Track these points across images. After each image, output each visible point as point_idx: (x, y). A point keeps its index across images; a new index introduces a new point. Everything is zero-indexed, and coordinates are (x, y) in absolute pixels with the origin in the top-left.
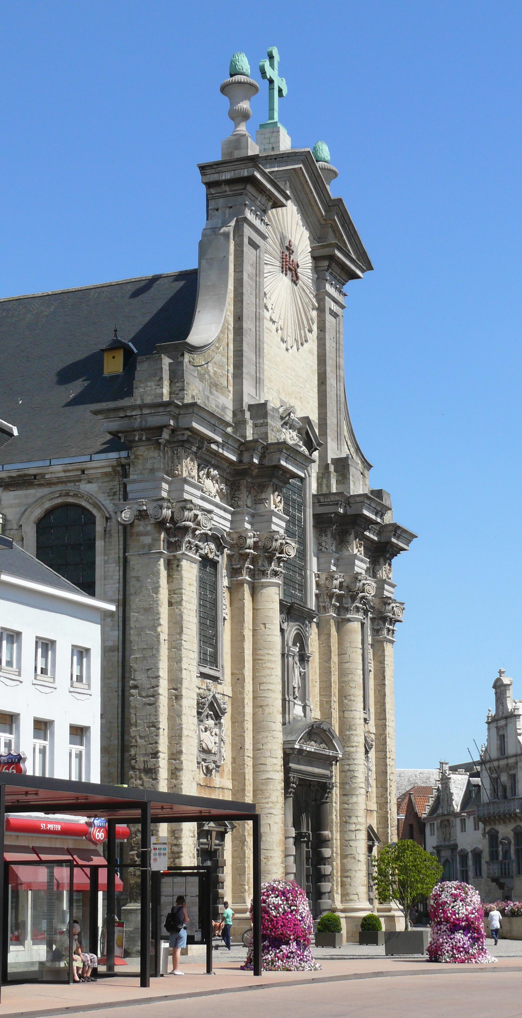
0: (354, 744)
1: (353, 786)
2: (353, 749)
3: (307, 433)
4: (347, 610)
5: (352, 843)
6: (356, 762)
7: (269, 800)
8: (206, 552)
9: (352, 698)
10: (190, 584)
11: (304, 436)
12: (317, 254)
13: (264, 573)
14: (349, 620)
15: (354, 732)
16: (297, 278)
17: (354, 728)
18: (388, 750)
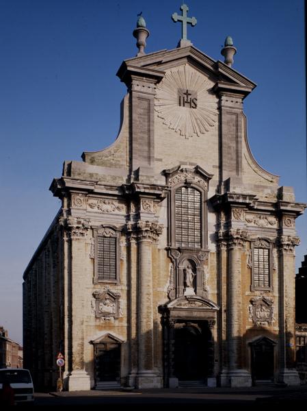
14: (232, 249)
16: (196, 105)
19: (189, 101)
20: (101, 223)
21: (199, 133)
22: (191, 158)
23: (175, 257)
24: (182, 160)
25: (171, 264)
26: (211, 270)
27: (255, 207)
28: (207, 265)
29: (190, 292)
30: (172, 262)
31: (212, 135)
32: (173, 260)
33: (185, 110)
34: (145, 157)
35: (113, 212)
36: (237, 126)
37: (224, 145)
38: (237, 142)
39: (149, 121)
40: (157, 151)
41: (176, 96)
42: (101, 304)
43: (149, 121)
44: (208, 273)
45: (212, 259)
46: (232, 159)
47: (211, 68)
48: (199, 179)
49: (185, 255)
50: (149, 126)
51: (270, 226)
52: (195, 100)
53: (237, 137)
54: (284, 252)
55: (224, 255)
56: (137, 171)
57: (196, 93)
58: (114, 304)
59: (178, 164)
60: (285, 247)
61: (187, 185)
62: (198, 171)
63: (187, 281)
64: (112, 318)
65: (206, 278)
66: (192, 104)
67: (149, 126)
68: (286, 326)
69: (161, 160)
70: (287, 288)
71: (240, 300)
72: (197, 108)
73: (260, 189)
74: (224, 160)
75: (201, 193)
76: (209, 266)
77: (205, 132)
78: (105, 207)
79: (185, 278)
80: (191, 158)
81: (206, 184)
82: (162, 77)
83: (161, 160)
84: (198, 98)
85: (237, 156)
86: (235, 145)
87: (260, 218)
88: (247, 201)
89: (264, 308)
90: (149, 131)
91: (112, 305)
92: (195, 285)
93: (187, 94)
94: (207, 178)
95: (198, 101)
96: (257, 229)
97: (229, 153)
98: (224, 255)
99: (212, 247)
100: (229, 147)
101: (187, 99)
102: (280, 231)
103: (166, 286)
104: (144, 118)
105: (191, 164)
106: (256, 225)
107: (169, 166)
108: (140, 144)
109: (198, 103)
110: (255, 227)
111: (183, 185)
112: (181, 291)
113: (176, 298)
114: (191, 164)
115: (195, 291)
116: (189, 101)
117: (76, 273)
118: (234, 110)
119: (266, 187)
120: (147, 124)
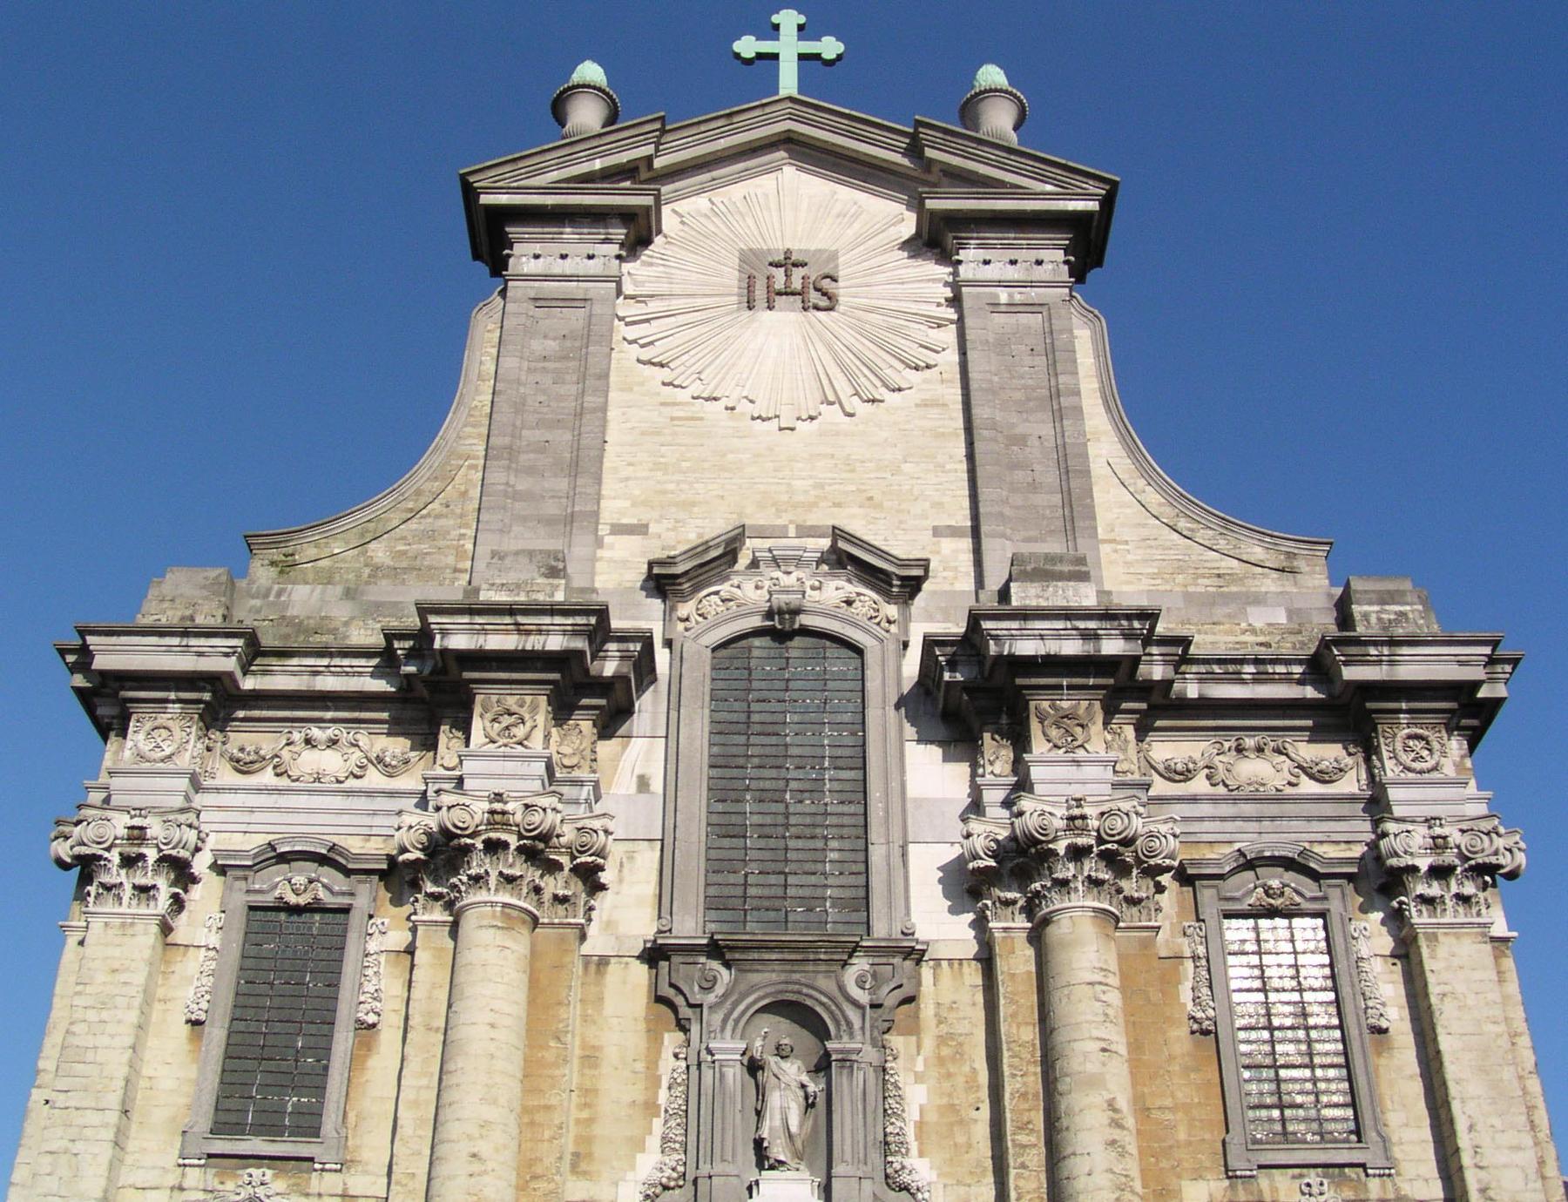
8: (277, 893)
19: (797, 284)
20: (262, 840)
21: (854, 404)
22: (812, 506)
23: (697, 997)
24: (755, 519)
25: (672, 1039)
26: (941, 1061)
27: (1192, 691)
28: (914, 1029)
30: (682, 1026)
31: (925, 404)
32: (685, 1012)
33: (785, 321)
34: (549, 522)
35: (352, 783)
36: (1051, 352)
38: (1059, 415)
44: (919, 1078)
45: (949, 994)
46: (1034, 487)
47: (905, 162)
48: (853, 589)
49: (755, 978)
51: (1308, 787)
52: (826, 284)
54: (1419, 917)
55: (1017, 961)
57: (834, 256)
60: (1421, 889)
61: (782, 627)
62: (845, 557)
65: (912, 1114)
66: (814, 297)
69: (640, 529)
70: (1484, 1138)
72: (841, 308)
73: (1219, 612)
75: (859, 651)
76: (928, 1042)
77: (882, 393)
78: (310, 761)
80: (812, 506)
81: (892, 610)
83: (640, 529)
84: (842, 273)
85: (1065, 472)
86: (1047, 430)
87: (1240, 750)
88: (1112, 646)
93: (788, 262)
94: (904, 584)
95: (841, 284)
96: (1226, 809)
98: (1017, 961)
99: (942, 927)
101: (791, 282)
102: (1376, 804)
105: (805, 531)
106: (1221, 790)
107: (678, 536)
108: (531, 471)
109: (842, 290)
110: (1214, 800)
111: (756, 622)
114: (805, 531)
118: (1033, 294)
119: (1258, 600)
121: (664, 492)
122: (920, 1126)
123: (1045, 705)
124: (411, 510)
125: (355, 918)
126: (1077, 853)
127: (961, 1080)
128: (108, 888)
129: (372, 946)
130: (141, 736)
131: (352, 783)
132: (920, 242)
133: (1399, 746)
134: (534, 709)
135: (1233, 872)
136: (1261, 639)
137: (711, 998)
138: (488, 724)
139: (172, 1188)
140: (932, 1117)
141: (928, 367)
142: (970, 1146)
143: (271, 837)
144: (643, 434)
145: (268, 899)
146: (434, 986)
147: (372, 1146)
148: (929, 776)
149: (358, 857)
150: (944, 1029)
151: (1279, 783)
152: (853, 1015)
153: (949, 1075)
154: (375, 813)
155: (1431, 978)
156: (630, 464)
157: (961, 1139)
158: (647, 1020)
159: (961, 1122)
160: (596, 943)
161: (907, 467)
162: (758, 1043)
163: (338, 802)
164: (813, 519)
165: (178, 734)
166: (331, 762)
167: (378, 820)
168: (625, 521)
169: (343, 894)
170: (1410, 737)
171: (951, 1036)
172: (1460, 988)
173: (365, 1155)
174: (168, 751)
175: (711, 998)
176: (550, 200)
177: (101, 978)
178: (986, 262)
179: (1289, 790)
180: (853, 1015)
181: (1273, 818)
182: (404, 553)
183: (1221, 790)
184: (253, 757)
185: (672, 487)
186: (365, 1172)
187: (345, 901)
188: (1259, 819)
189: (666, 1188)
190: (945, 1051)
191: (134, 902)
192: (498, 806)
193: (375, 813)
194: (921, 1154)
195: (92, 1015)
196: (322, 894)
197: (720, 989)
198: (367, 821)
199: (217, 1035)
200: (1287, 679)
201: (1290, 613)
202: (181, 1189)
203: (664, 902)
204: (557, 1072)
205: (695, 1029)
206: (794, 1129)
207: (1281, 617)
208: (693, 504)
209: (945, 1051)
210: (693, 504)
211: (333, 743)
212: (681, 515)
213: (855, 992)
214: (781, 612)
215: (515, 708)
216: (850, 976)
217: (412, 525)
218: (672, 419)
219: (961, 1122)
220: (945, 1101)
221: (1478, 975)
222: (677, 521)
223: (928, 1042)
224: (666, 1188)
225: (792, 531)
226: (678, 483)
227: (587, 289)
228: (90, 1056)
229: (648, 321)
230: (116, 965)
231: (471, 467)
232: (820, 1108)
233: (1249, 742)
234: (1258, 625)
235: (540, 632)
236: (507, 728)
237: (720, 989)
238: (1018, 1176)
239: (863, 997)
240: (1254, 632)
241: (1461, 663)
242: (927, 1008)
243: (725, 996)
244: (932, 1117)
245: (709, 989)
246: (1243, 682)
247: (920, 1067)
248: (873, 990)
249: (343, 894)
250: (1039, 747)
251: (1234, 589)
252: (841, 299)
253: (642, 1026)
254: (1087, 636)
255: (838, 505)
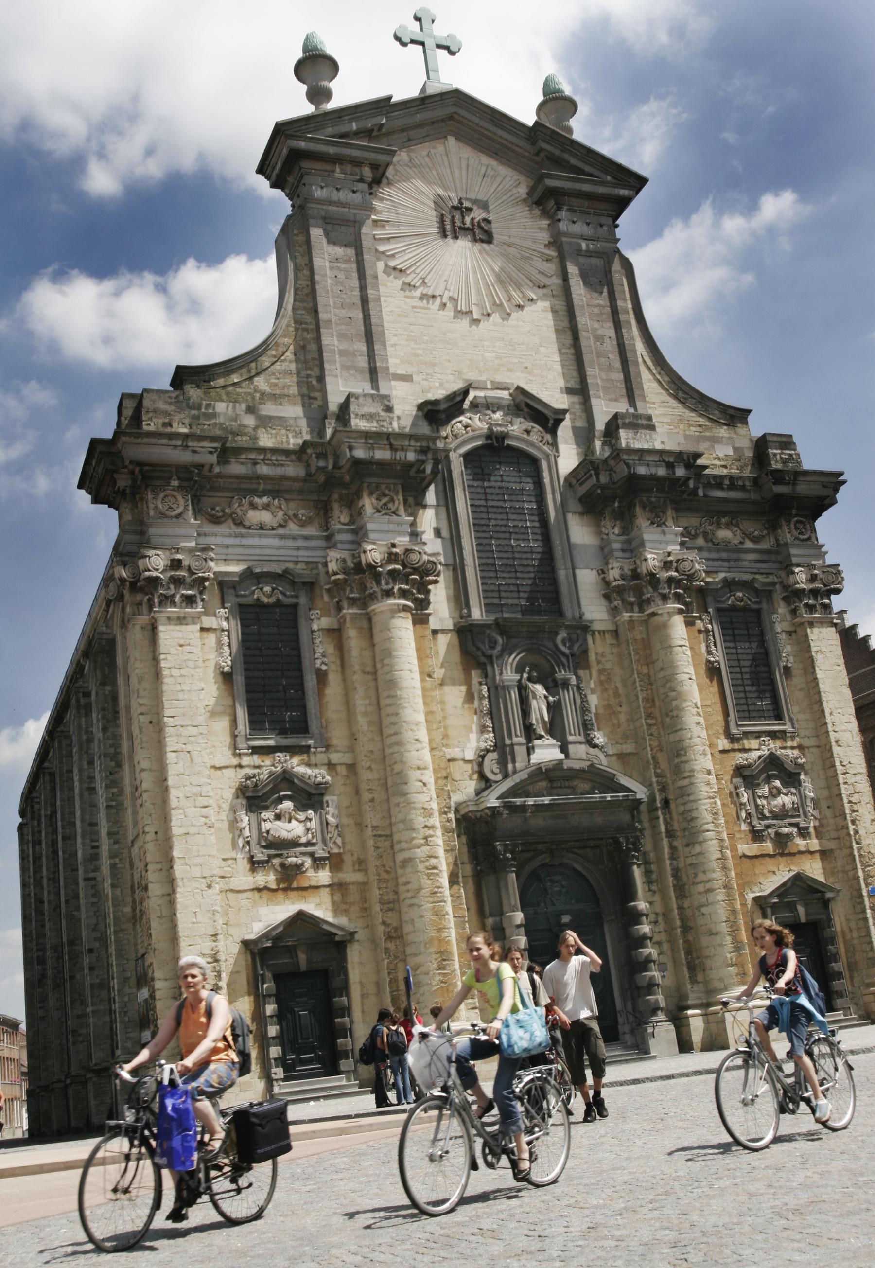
0: (686, 774)
1: (694, 830)
2: (686, 782)
3: (528, 405)
4: (649, 601)
5: (704, 910)
6: (691, 798)
7: (409, 887)
9: (675, 713)
10: (181, 646)
11: (526, 410)
12: (536, 197)
13: (372, 597)
15: (684, 759)
17: (682, 752)
18: (837, 763)
19: (468, 224)
23: (489, 652)
24: (473, 376)
26: (601, 683)
28: (587, 667)
29: (547, 752)
33: (463, 246)
37: (583, 335)
38: (618, 326)
39: (362, 276)
40: (395, 356)
41: (432, 215)
42: (265, 815)
43: (362, 276)
44: (593, 691)
46: (610, 368)
48: (529, 425)
50: (363, 288)
51: (749, 545)
53: (615, 312)
56: (345, 407)
58: (311, 813)
59: (458, 386)
63: (534, 718)
64: (308, 862)
65: (593, 710)
67: (363, 288)
68: (856, 832)
69: (407, 378)
71: (709, 765)
72: (495, 242)
74: (589, 371)
76: (595, 674)
78: (255, 516)
79: (526, 712)
82: (387, 165)
86: (612, 333)
89: (778, 783)
90: (365, 301)
91: (302, 816)
92: (556, 728)
95: (493, 225)
97: (599, 355)
100: (599, 339)
103: (471, 742)
104: (345, 270)
107: (439, 390)
108: (342, 336)
112: (520, 751)
113: (506, 776)
115: (564, 749)
116: (468, 224)
117: (178, 721)
120: (356, 283)
121: (417, 355)
122: (596, 715)
123: (644, 499)
124: (275, 356)
125: (301, 611)
126: (670, 580)
127: (611, 692)
128: (166, 597)
129: (315, 627)
130: (159, 502)
131: (281, 531)
132: (530, 201)
133: (792, 526)
134: (397, 494)
135: (722, 588)
136: (723, 463)
137: (495, 652)
138: (374, 501)
139: (236, 767)
140: (601, 711)
141: (544, 287)
142: (619, 725)
143: (250, 564)
144: (399, 315)
145: (249, 601)
146: (362, 649)
147: (338, 735)
148: (580, 532)
149: (300, 576)
150: (601, 666)
151: (736, 542)
152: (564, 660)
153: (606, 690)
154: (299, 549)
155: (812, 644)
156: (395, 335)
157: (615, 722)
158: (462, 663)
159: (614, 713)
160: (433, 624)
161: (542, 349)
162: (525, 676)
163: (276, 542)
164: (499, 378)
165: (181, 501)
166: (265, 517)
167: (301, 553)
168: (399, 372)
169: (292, 596)
170: (797, 522)
171: (604, 670)
172: (824, 649)
173: (335, 742)
174: (178, 511)
175: (495, 652)
176: (332, 150)
177: (173, 651)
178: (574, 222)
179: (741, 546)
180: (564, 660)
181: (735, 560)
182: (276, 385)
183: (710, 545)
184: (221, 514)
185: (420, 352)
186: (337, 751)
187: (294, 600)
188: (728, 560)
189: (488, 751)
190: (603, 678)
191: (184, 604)
192: (394, 550)
193: (299, 549)
194: (599, 730)
195: (176, 672)
196: (280, 596)
197: (499, 648)
198: (295, 553)
199: (239, 679)
200: (743, 488)
201: (735, 449)
202: (240, 766)
203: (460, 597)
204: (433, 694)
205: (489, 668)
206: (547, 719)
207: (731, 452)
208: (434, 365)
209: (603, 678)
210: (434, 365)
211: (266, 507)
212: (430, 371)
213: (562, 648)
214: (497, 438)
215: (387, 492)
216: (559, 639)
217: (277, 366)
218: (414, 307)
219: (614, 713)
220: (605, 703)
221: (830, 642)
222: (428, 374)
223: (595, 674)
224: (488, 751)
225: (489, 387)
226: (424, 349)
227: (355, 215)
228: (181, 696)
229: (389, 239)
230: (182, 642)
231: (307, 330)
232: (555, 709)
233: (723, 520)
234: (721, 455)
235: (402, 449)
236: (385, 504)
237: (499, 648)
238: (650, 740)
239: (567, 651)
240: (719, 459)
241: (824, 486)
242: (592, 657)
243: (503, 651)
244: (601, 711)
245: (493, 648)
246: (723, 489)
247: (592, 686)
248: (570, 648)
249: (292, 596)
250: (642, 522)
251: (707, 434)
252: (495, 236)
253: (460, 667)
254: (670, 466)
255: (510, 370)
